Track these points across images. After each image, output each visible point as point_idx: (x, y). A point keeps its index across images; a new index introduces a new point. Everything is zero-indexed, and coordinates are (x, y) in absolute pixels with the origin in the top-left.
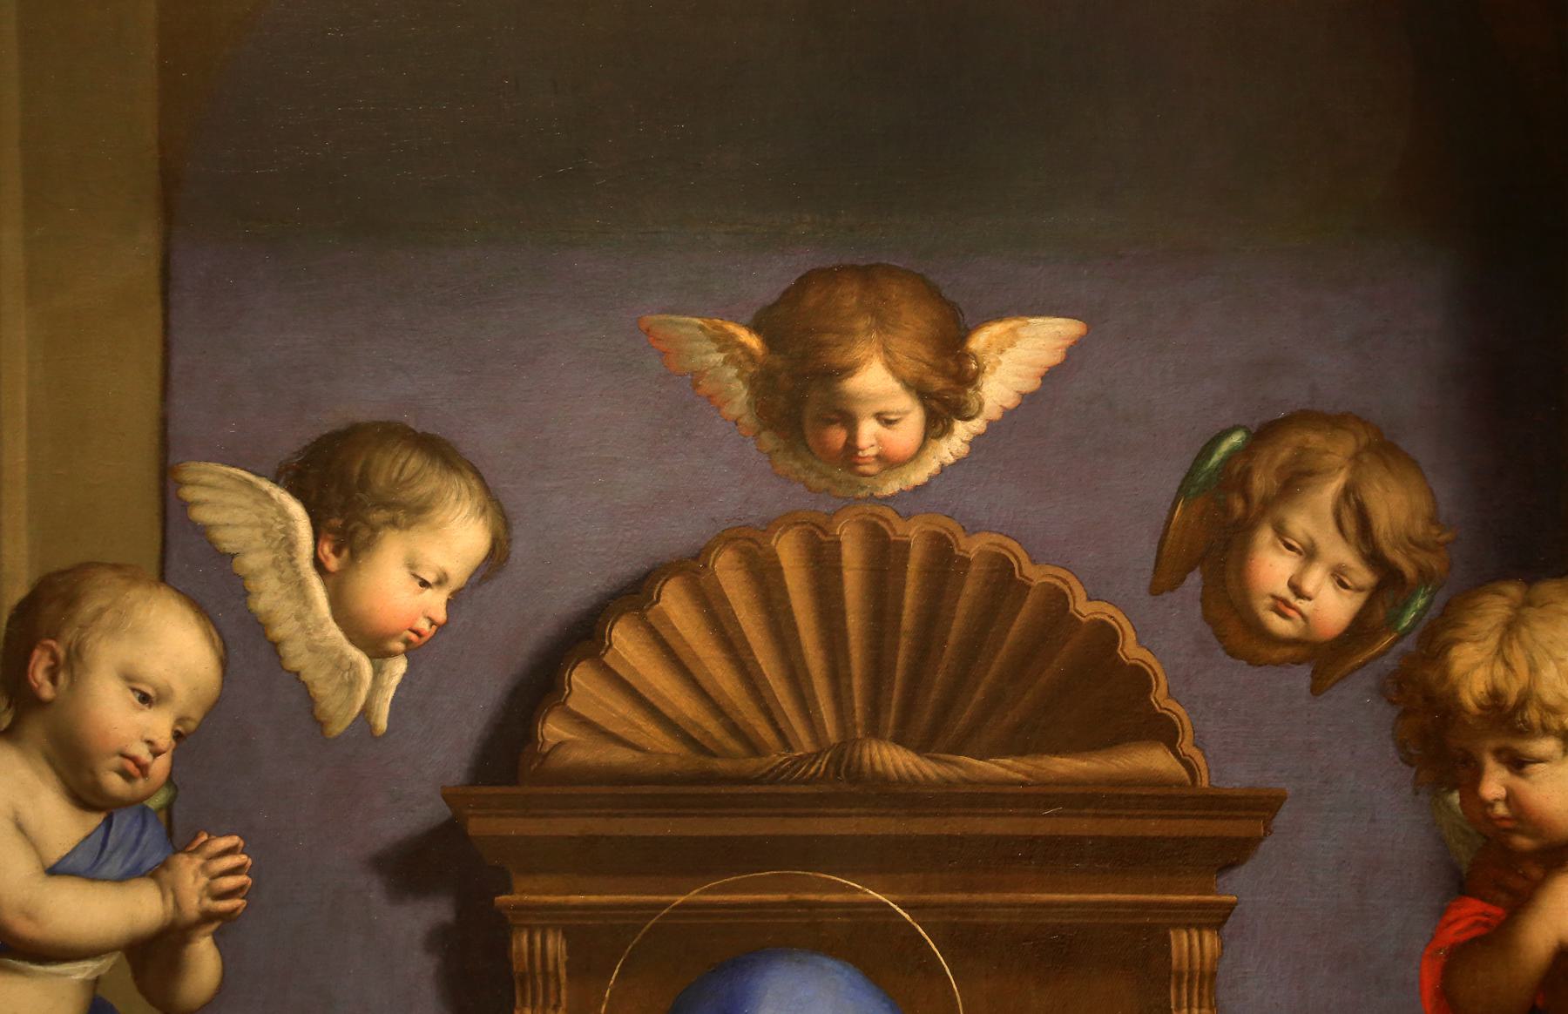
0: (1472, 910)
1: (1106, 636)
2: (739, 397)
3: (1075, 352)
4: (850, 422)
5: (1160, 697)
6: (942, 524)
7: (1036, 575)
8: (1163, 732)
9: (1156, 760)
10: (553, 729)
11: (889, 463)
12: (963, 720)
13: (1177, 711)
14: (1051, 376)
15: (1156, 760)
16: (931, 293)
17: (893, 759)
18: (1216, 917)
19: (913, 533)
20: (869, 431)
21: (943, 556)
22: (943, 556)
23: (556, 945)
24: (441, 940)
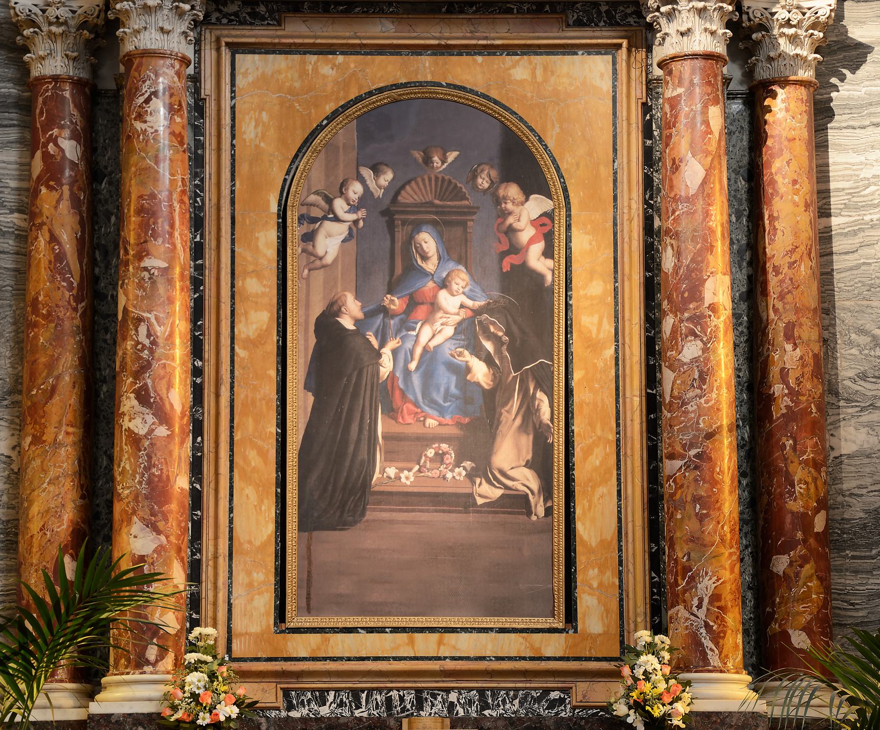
0: (500, 220)
1: (461, 188)
2: (420, 160)
3: (458, 156)
4: (433, 163)
5: (467, 195)
6: (443, 175)
7: (453, 181)
8: (467, 199)
9: (466, 203)
10: (399, 198)
11: (437, 168)
12: (445, 198)
13: (469, 197)
14: (456, 158)
15: (466, 203)
16: (442, 148)
17: (437, 202)
18: (473, 220)
19: (440, 176)
20: (435, 164)
21: (443, 178)
22: (443, 178)
23: (400, 222)
24: (387, 221)
